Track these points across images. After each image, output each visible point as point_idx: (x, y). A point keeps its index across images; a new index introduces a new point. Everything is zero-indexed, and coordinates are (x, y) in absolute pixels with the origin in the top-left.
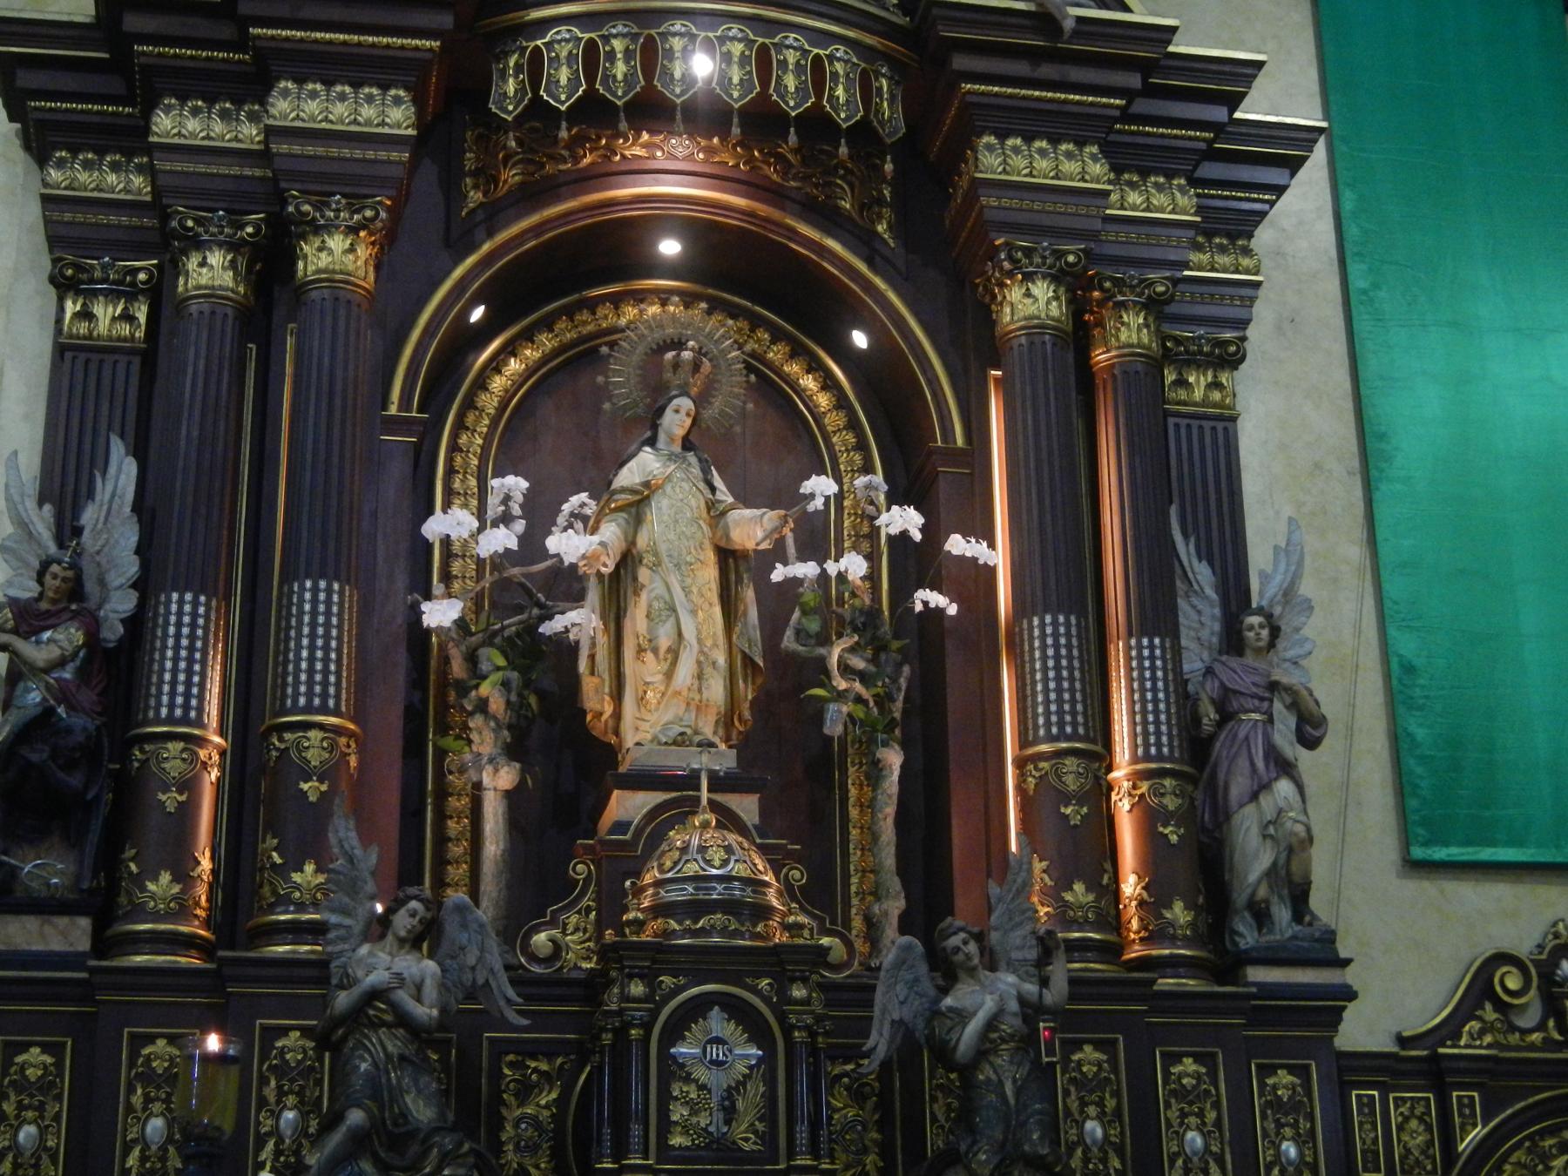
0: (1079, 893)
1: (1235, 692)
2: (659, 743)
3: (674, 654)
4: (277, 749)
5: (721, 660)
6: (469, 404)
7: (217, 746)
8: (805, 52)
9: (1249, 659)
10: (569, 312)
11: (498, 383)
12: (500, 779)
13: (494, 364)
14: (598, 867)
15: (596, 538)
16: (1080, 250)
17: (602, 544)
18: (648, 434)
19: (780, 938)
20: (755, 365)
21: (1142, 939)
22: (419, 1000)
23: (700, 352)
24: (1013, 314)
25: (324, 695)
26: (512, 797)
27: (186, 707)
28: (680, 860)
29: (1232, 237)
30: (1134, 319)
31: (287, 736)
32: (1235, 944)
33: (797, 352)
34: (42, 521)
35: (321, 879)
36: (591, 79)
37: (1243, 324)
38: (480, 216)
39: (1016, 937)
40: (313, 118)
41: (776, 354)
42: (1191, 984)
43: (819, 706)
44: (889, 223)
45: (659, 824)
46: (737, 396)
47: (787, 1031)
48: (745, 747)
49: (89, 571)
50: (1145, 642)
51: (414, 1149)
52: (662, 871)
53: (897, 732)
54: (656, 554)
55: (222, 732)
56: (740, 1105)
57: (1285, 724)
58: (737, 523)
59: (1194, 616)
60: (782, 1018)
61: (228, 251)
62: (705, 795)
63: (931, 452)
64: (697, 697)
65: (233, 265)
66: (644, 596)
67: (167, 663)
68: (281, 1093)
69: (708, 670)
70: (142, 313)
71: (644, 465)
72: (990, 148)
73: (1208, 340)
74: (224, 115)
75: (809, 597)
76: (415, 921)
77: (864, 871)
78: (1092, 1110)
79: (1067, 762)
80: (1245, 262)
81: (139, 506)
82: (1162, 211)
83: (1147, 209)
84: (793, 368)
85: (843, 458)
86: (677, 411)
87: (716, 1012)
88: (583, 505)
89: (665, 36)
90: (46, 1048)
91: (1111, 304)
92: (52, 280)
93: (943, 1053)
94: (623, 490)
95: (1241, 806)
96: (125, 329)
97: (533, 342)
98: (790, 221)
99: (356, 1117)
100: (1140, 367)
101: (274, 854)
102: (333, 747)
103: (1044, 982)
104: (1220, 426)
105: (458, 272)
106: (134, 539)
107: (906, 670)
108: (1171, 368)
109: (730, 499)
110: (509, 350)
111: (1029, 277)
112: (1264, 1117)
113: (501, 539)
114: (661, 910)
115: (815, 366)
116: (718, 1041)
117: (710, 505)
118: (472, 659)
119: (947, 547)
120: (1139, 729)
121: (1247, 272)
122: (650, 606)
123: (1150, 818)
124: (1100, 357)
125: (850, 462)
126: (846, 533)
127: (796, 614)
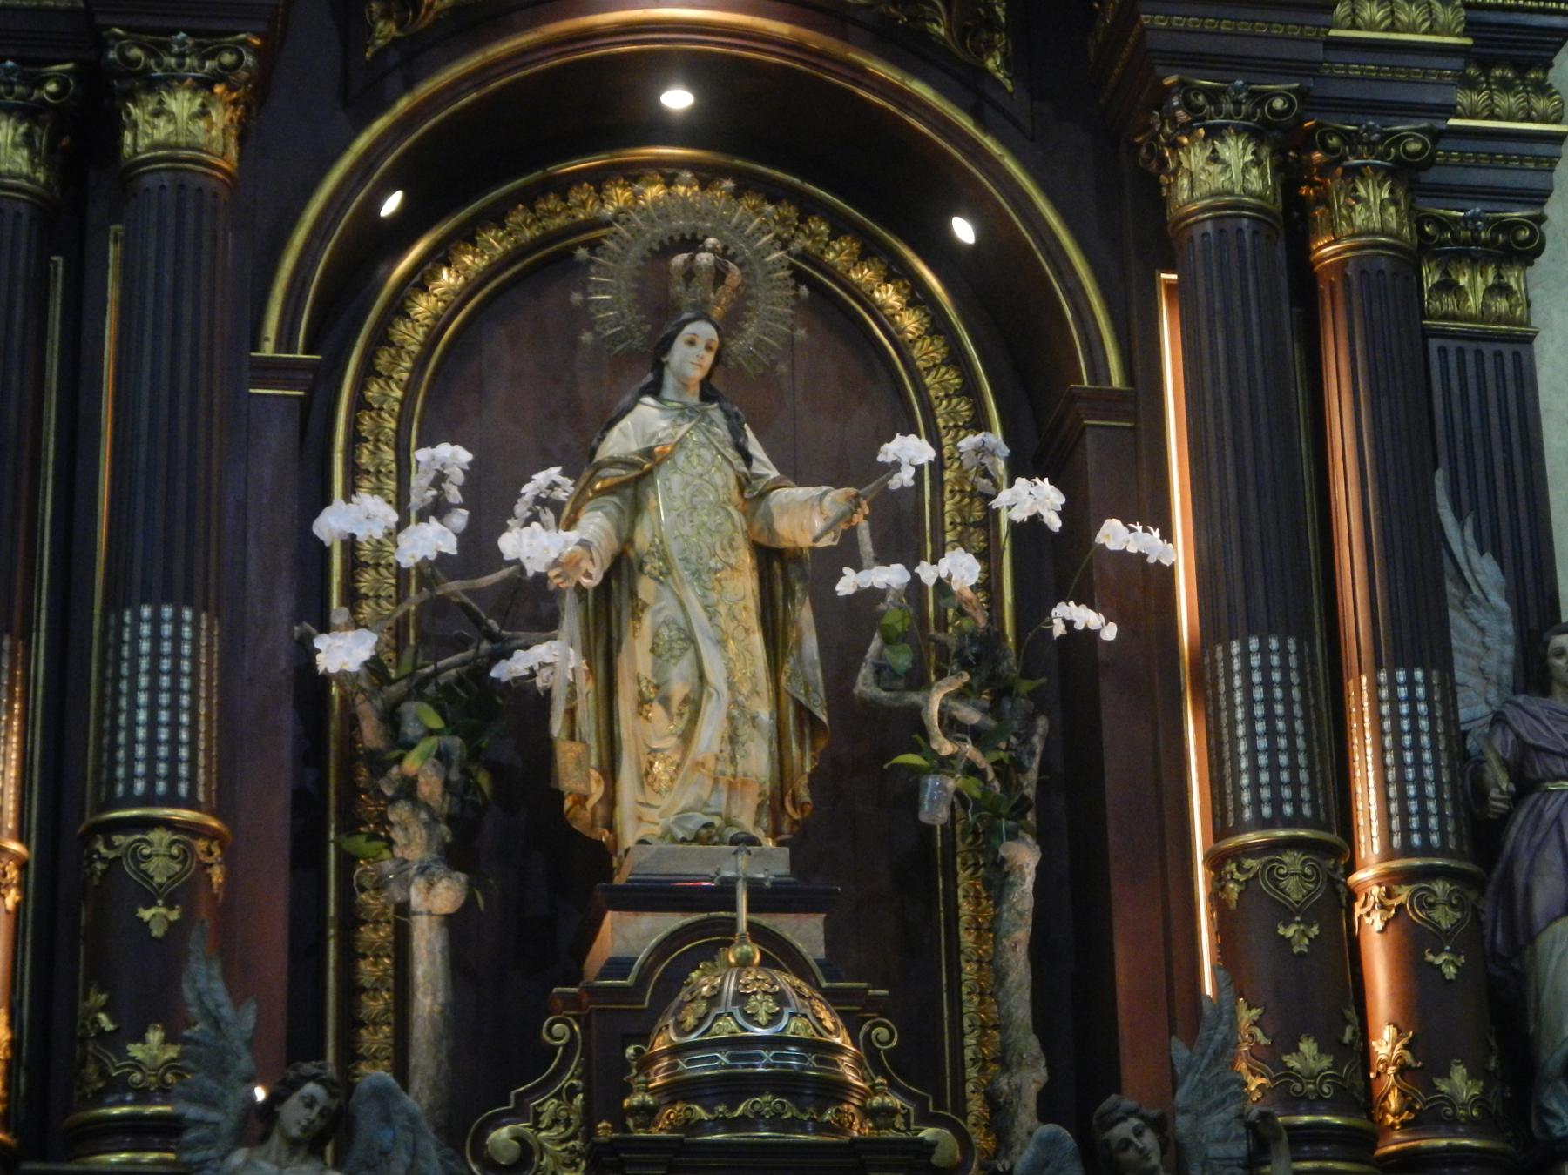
0: (1308, 1055)
1: (1538, 749)
2: (674, 840)
3: (694, 705)
4: (103, 859)
5: (765, 713)
6: (382, 338)
7: (14, 856)
10: (529, 197)
11: (423, 307)
13: (417, 279)
14: (585, 1027)
15: (573, 535)
16: (1290, 90)
17: (583, 543)
18: (650, 377)
19: (859, 1129)
21: (1404, 1124)
23: (724, 254)
24: (1192, 189)
25: (173, 778)
26: (453, 924)
28: (706, 1015)
29: (1521, 67)
30: (1375, 193)
31: (119, 839)
32: (1547, 1129)
33: (870, 250)
35: (172, 1052)
37: (1539, 197)
38: (393, 58)
39: (1215, 1122)
41: (839, 254)
44: (1004, 55)
46: (779, 318)
48: (800, 844)
50: (1401, 676)
52: (681, 1032)
53: (1030, 817)
54: (664, 558)
55: (21, 835)
58: (785, 509)
59: (1473, 634)
61: (20, 120)
62: (743, 916)
63: (1074, 397)
64: (729, 770)
66: (647, 621)
69: (745, 730)
73: (1488, 223)
75: (894, 617)
76: (314, 1114)
77: (984, 1027)
79: (1286, 859)
80: (1541, 104)
82: (1413, 29)
83: (1392, 28)
84: (864, 275)
86: (692, 343)
88: (553, 486)
91: (1339, 170)
94: (614, 462)
95: (1553, 920)
97: (475, 244)
98: (856, 56)
100: (1384, 265)
101: (102, 1017)
102: (187, 854)
104: (1507, 350)
105: (362, 142)
107: (1042, 723)
108: (1433, 265)
109: (774, 473)
110: (440, 256)
111: (1215, 133)
114: (679, 1090)
115: (897, 272)
117: (744, 483)
118: (391, 718)
119: (1100, 538)
120: (1394, 807)
121: (1544, 119)
122: (656, 635)
124: (1326, 250)
125: (953, 414)
126: (948, 520)
127: (876, 644)
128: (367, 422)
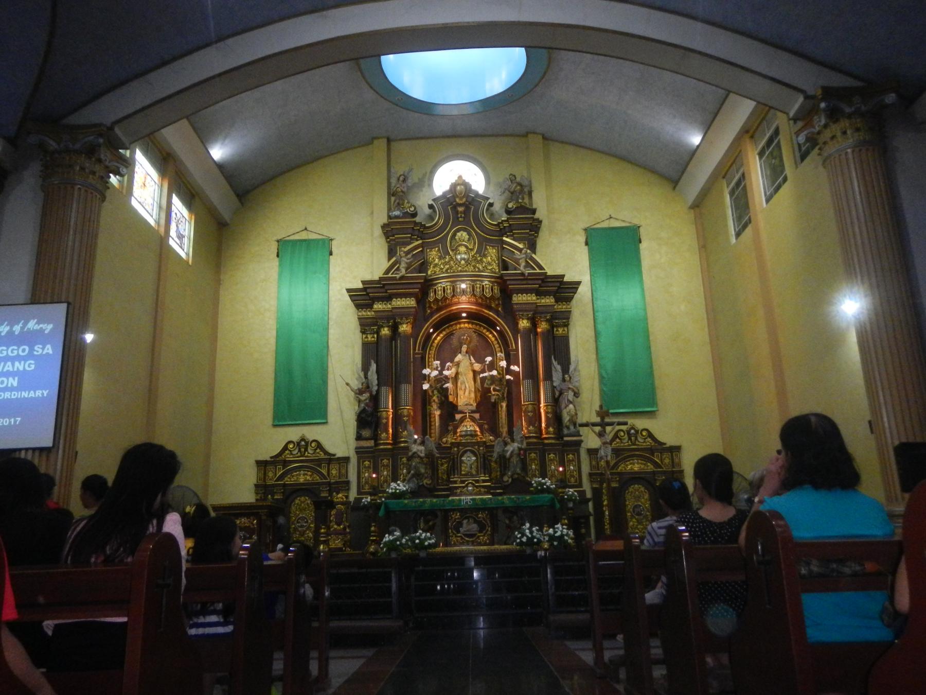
3: (465, 390)
5: (473, 390)
6: (431, 346)
8: (480, 285)
9: (566, 383)
10: (448, 327)
11: (436, 342)
12: (438, 413)
17: (452, 373)
19: (479, 440)
20: (481, 335)
22: (421, 453)
25: (407, 403)
26: (440, 416)
27: (386, 406)
29: (566, 302)
31: (402, 410)
33: (488, 330)
34: (362, 374)
36: (444, 294)
40: (399, 305)
42: (553, 441)
43: (490, 396)
45: (462, 420)
47: (480, 455)
49: (369, 382)
51: (421, 476)
53: (506, 399)
56: (473, 466)
57: (570, 395)
60: (478, 452)
62: (468, 414)
65: (389, 330)
66: (460, 381)
67: (382, 399)
68: (403, 467)
70: (376, 336)
71: (459, 357)
72: (515, 297)
74: (385, 304)
78: (533, 464)
80: (568, 307)
81: (377, 372)
84: (487, 333)
85: (497, 349)
87: (468, 452)
89: (456, 285)
90: (369, 461)
92: (361, 332)
93: (504, 457)
95: (564, 409)
96: (373, 339)
98: (484, 310)
99: (412, 472)
102: (408, 412)
103: (522, 444)
105: (426, 326)
106: (376, 377)
107: (507, 388)
110: (438, 335)
111: (523, 319)
112: (567, 462)
113: (435, 373)
114: (461, 436)
115: (491, 333)
116: (469, 457)
117: (470, 363)
118: (433, 392)
123: (546, 413)
124: (539, 330)
128: (430, 356)
